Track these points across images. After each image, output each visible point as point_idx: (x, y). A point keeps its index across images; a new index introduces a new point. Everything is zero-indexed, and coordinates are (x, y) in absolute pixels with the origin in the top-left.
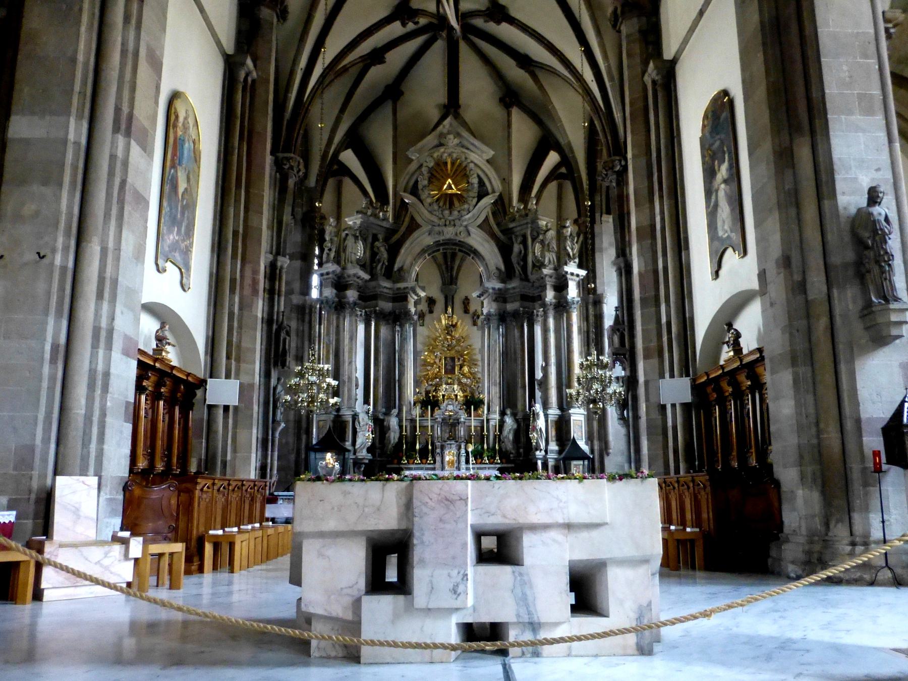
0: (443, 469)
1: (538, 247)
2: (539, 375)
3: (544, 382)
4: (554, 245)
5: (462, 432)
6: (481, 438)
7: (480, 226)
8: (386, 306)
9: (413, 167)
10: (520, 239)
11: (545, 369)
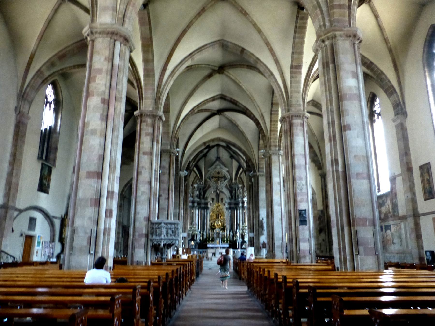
0: (216, 244)
1: (238, 193)
2: (238, 222)
3: (239, 224)
4: (242, 193)
5: (220, 236)
6: (225, 237)
7: (225, 187)
8: (203, 206)
9: (210, 172)
10: (234, 190)
11: (239, 221)
